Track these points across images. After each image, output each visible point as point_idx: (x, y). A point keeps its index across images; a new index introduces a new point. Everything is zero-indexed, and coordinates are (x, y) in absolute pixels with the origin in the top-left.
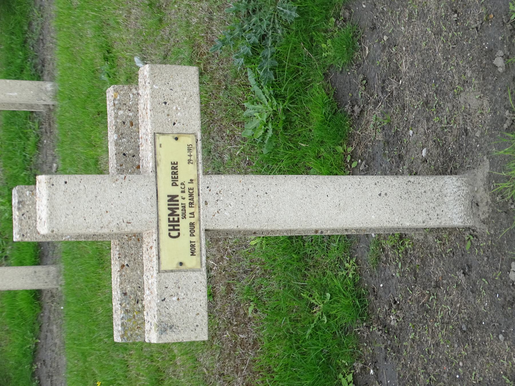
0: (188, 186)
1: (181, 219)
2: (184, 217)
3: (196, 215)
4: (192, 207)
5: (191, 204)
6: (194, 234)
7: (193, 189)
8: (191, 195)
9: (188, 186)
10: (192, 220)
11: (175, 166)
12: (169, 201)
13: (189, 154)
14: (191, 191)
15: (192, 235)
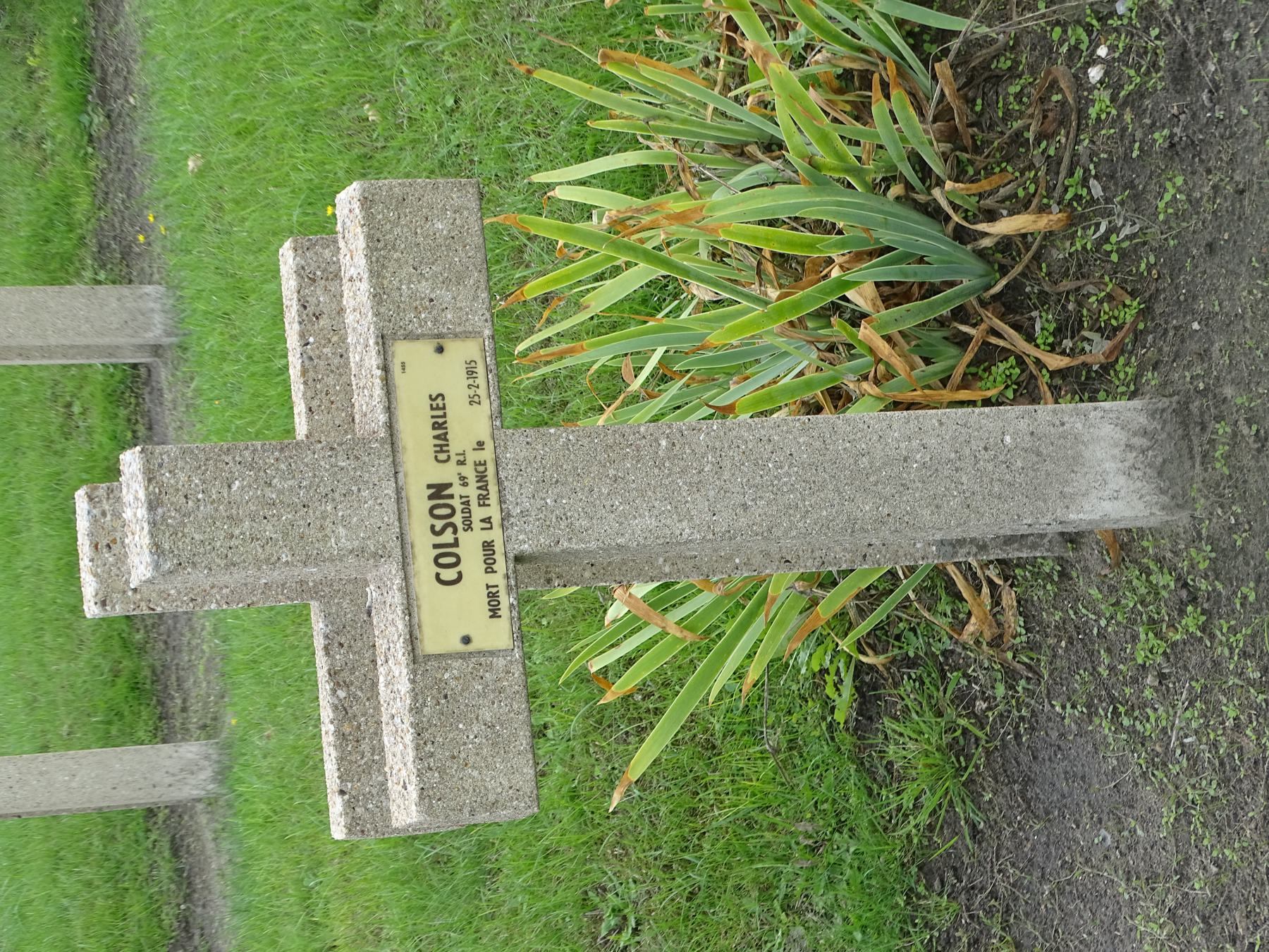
0: (472, 457)
1: (461, 534)
2: (469, 527)
3: (496, 520)
4: (484, 505)
5: (483, 500)
6: (495, 567)
7: (485, 464)
8: (481, 477)
9: (472, 457)
10: (487, 536)
11: (440, 413)
12: (430, 497)
13: (471, 382)
14: (481, 468)
15: (490, 570)
